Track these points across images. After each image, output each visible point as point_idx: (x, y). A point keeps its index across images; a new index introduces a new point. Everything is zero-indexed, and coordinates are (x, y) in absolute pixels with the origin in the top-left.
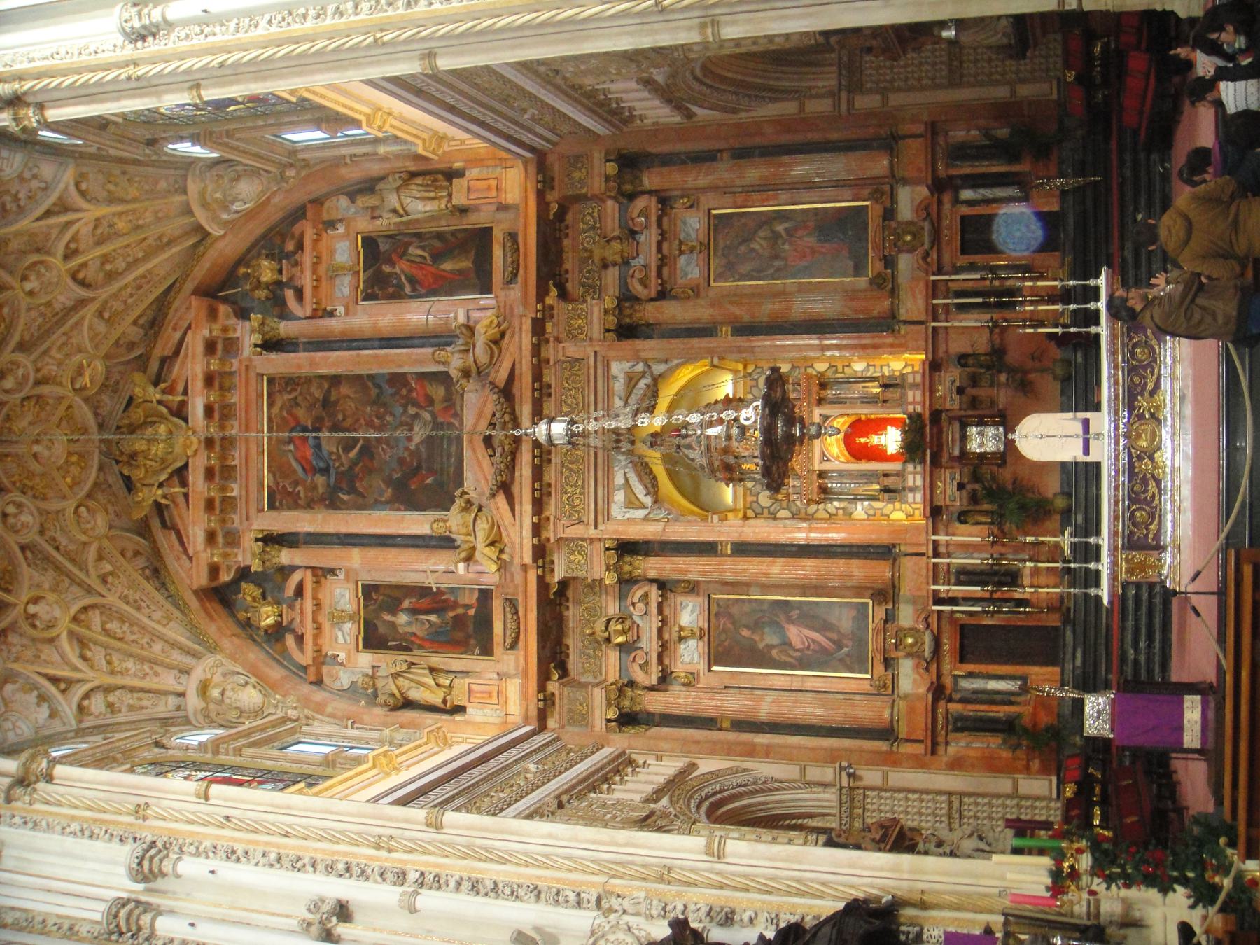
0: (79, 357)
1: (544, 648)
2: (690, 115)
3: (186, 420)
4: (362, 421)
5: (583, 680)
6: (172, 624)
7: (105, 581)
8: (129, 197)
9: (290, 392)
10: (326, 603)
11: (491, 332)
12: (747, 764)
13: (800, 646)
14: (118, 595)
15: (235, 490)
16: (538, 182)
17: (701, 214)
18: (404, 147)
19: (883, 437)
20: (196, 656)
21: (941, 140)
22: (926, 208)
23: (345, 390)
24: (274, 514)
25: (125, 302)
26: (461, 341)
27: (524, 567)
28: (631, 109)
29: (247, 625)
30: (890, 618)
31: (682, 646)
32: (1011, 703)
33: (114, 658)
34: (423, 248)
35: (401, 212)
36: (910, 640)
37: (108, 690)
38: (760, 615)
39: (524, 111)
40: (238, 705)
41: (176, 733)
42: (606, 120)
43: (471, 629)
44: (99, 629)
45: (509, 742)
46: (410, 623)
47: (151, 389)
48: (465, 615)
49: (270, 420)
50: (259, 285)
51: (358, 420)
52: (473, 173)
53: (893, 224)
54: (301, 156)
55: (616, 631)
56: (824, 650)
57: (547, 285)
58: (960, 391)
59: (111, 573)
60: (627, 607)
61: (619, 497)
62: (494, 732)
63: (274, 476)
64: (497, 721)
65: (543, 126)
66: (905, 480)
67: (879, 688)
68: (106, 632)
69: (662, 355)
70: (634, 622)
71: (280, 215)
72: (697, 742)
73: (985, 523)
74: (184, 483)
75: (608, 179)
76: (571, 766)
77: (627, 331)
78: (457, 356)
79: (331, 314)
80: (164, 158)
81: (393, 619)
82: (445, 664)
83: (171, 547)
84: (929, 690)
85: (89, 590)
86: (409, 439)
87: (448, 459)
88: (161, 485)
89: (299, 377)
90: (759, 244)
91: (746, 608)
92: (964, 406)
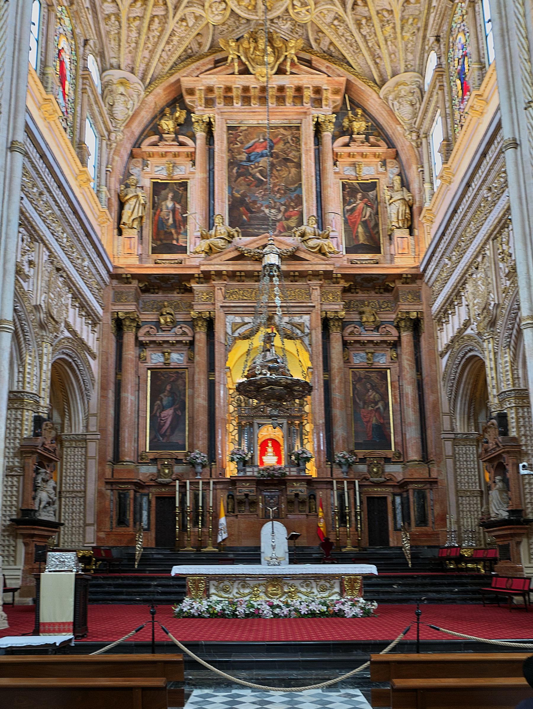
4: (277, 180)
5: (140, 301)
7: (183, 20)
9: (292, 140)
10: (178, 160)
14: (175, 29)
19: (272, 454)
23: (293, 170)
24: (225, 129)
25: (343, 36)
28: (447, 322)
40: (116, 104)
43: (165, 242)
46: (167, 208)
48: (173, 239)
49: (277, 128)
51: (277, 178)
54: (424, 140)
55: (166, 318)
57: (350, 281)
58: (297, 495)
59: (187, 26)
60: (179, 325)
61: (238, 320)
63: (245, 130)
64: (115, 253)
66: (250, 467)
69: (314, 341)
70: (172, 328)
77: (326, 323)
80: (426, 55)
81: (169, 199)
82: (146, 227)
83: (204, 65)
86: (267, 207)
87: (256, 228)
89: (300, 145)
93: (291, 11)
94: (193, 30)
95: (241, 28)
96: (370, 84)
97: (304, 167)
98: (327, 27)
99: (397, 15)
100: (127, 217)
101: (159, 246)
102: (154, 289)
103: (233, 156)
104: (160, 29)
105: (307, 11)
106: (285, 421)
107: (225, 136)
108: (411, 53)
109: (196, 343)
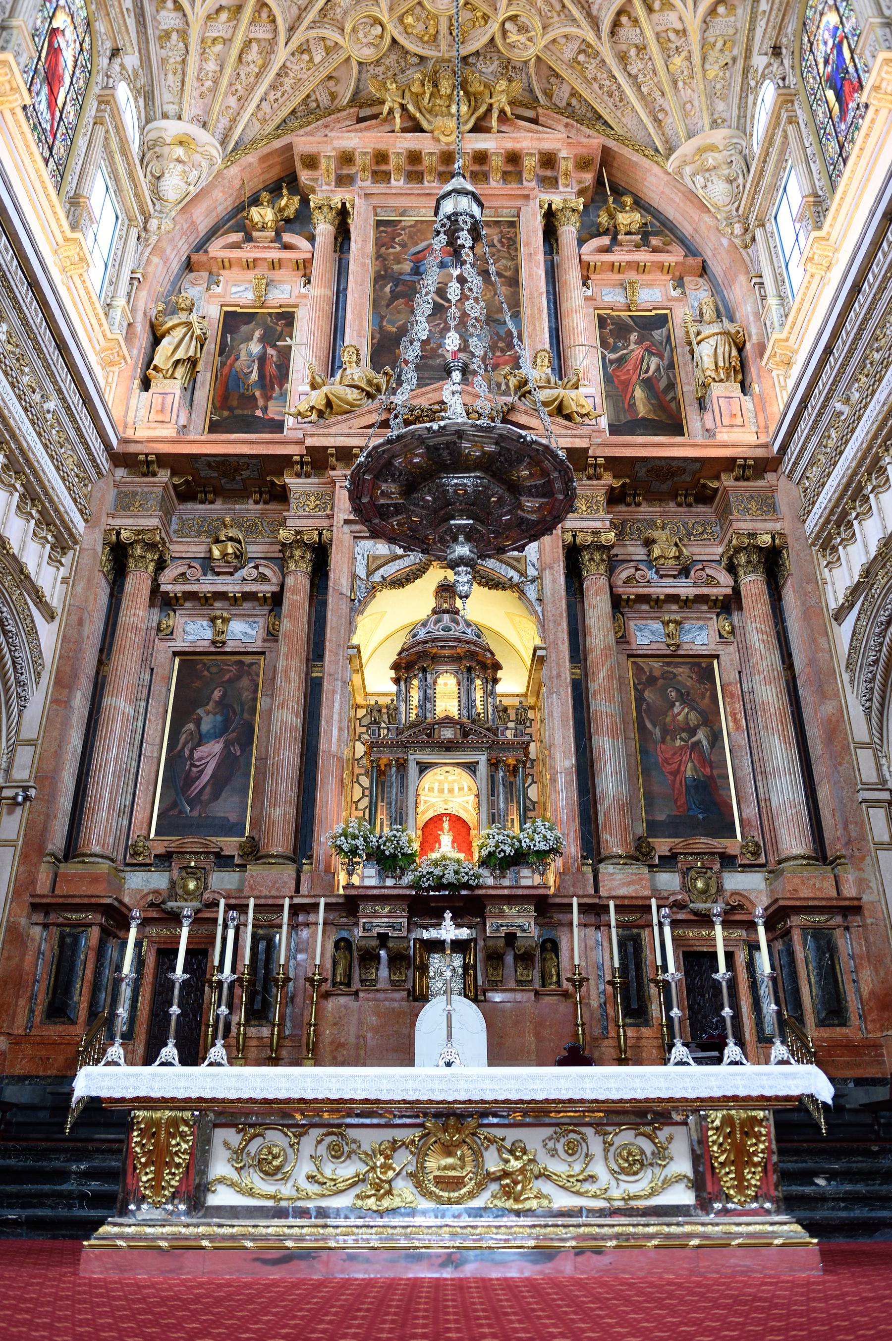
0: (539, 25)
1: (209, 465)
2: (839, 616)
3: (471, 131)
6: (257, 125)
7: (304, 49)
8: (707, 66)
9: (500, 242)
10: (277, 275)
11: (573, 404)
12: (46, 678)
13: (197, 755)
14: (288, 64)
15: (398, 183)
16: (745, 459)
17: (712, 646)
18: (776, 324)
20: (223, 143)
21: (838, 920)
22: (741, 906)
26: (560, 383)
27: (300, 442)
29: (255, 201)
30: (223, 861)
31: (205, 623)
32: (93, 1013)
33: (218, 48)
34: (658, 369)
35: (699, 338)
36: (192, 885)
37: (184, 35)
38: (238, 711)
39: (847, 401)
40: (166, 175)
41: (136, 100)
42: (832, 512)
43: (238, 412)
44: (252, 36)
45: (55, 321)
46: (250, 354)
47: (504, 98)
48: (257, 407)
50: (612, 217)
52: (748, 403)
53: (717, 867)
54: (759, 233)
55: (226, 548)
56: (190, 781)
59: (311, 60)
62: (116, 414)
63: (411, 226)
65: (820, 444)
67: (135, 845)
68: (248, 43)
69: (548, 591)
70: (237, 569)
71: (687, 229)
72: (81, 623)
73: (334, 975)
74: (404, 130)
75: (752, 535)
76: (51, 457)
78: (544, 376)
79: (585, 284)
80: (751, 98)
82: (203, 385)
84: (121, 902)
85: (292, 29)
88: (403, 107)
89: (516, 250)
90: (681, 713)
91: (246, 695)
92: (490, 943)
93: (499, 41)
94: (321, 69)
95: (408, 72)
96: (647, 153)
97: (524, 281)
98: (564, 67)
99: (695, 37)
100: (163, 358)
101: (226, 419)
102: (206, 493)
103: (385, 266)
104: (260, 62)
105: (530, 39)
106: (482, 758)
107: (371, 233)
108: (723, 100)
109: (287, 595)
